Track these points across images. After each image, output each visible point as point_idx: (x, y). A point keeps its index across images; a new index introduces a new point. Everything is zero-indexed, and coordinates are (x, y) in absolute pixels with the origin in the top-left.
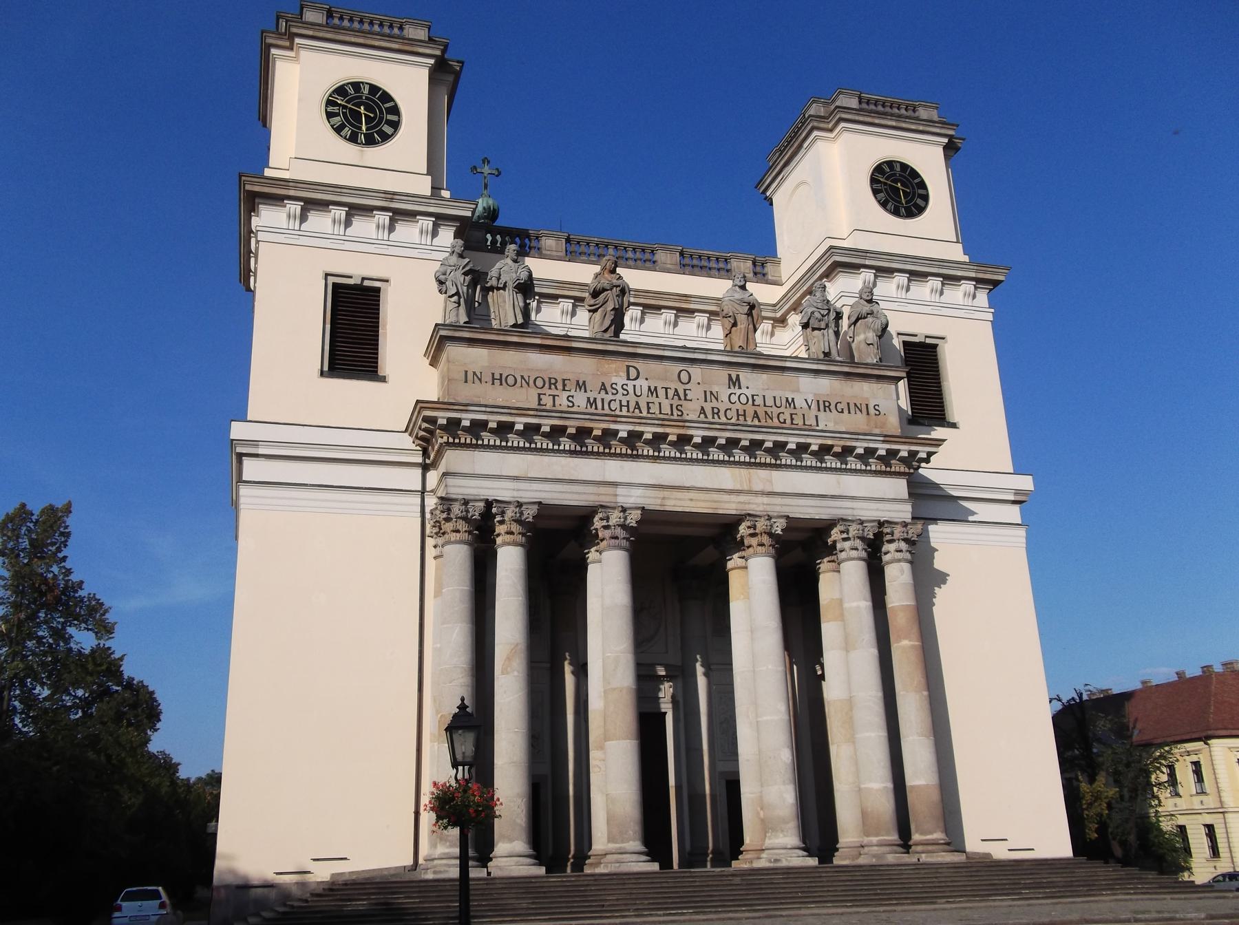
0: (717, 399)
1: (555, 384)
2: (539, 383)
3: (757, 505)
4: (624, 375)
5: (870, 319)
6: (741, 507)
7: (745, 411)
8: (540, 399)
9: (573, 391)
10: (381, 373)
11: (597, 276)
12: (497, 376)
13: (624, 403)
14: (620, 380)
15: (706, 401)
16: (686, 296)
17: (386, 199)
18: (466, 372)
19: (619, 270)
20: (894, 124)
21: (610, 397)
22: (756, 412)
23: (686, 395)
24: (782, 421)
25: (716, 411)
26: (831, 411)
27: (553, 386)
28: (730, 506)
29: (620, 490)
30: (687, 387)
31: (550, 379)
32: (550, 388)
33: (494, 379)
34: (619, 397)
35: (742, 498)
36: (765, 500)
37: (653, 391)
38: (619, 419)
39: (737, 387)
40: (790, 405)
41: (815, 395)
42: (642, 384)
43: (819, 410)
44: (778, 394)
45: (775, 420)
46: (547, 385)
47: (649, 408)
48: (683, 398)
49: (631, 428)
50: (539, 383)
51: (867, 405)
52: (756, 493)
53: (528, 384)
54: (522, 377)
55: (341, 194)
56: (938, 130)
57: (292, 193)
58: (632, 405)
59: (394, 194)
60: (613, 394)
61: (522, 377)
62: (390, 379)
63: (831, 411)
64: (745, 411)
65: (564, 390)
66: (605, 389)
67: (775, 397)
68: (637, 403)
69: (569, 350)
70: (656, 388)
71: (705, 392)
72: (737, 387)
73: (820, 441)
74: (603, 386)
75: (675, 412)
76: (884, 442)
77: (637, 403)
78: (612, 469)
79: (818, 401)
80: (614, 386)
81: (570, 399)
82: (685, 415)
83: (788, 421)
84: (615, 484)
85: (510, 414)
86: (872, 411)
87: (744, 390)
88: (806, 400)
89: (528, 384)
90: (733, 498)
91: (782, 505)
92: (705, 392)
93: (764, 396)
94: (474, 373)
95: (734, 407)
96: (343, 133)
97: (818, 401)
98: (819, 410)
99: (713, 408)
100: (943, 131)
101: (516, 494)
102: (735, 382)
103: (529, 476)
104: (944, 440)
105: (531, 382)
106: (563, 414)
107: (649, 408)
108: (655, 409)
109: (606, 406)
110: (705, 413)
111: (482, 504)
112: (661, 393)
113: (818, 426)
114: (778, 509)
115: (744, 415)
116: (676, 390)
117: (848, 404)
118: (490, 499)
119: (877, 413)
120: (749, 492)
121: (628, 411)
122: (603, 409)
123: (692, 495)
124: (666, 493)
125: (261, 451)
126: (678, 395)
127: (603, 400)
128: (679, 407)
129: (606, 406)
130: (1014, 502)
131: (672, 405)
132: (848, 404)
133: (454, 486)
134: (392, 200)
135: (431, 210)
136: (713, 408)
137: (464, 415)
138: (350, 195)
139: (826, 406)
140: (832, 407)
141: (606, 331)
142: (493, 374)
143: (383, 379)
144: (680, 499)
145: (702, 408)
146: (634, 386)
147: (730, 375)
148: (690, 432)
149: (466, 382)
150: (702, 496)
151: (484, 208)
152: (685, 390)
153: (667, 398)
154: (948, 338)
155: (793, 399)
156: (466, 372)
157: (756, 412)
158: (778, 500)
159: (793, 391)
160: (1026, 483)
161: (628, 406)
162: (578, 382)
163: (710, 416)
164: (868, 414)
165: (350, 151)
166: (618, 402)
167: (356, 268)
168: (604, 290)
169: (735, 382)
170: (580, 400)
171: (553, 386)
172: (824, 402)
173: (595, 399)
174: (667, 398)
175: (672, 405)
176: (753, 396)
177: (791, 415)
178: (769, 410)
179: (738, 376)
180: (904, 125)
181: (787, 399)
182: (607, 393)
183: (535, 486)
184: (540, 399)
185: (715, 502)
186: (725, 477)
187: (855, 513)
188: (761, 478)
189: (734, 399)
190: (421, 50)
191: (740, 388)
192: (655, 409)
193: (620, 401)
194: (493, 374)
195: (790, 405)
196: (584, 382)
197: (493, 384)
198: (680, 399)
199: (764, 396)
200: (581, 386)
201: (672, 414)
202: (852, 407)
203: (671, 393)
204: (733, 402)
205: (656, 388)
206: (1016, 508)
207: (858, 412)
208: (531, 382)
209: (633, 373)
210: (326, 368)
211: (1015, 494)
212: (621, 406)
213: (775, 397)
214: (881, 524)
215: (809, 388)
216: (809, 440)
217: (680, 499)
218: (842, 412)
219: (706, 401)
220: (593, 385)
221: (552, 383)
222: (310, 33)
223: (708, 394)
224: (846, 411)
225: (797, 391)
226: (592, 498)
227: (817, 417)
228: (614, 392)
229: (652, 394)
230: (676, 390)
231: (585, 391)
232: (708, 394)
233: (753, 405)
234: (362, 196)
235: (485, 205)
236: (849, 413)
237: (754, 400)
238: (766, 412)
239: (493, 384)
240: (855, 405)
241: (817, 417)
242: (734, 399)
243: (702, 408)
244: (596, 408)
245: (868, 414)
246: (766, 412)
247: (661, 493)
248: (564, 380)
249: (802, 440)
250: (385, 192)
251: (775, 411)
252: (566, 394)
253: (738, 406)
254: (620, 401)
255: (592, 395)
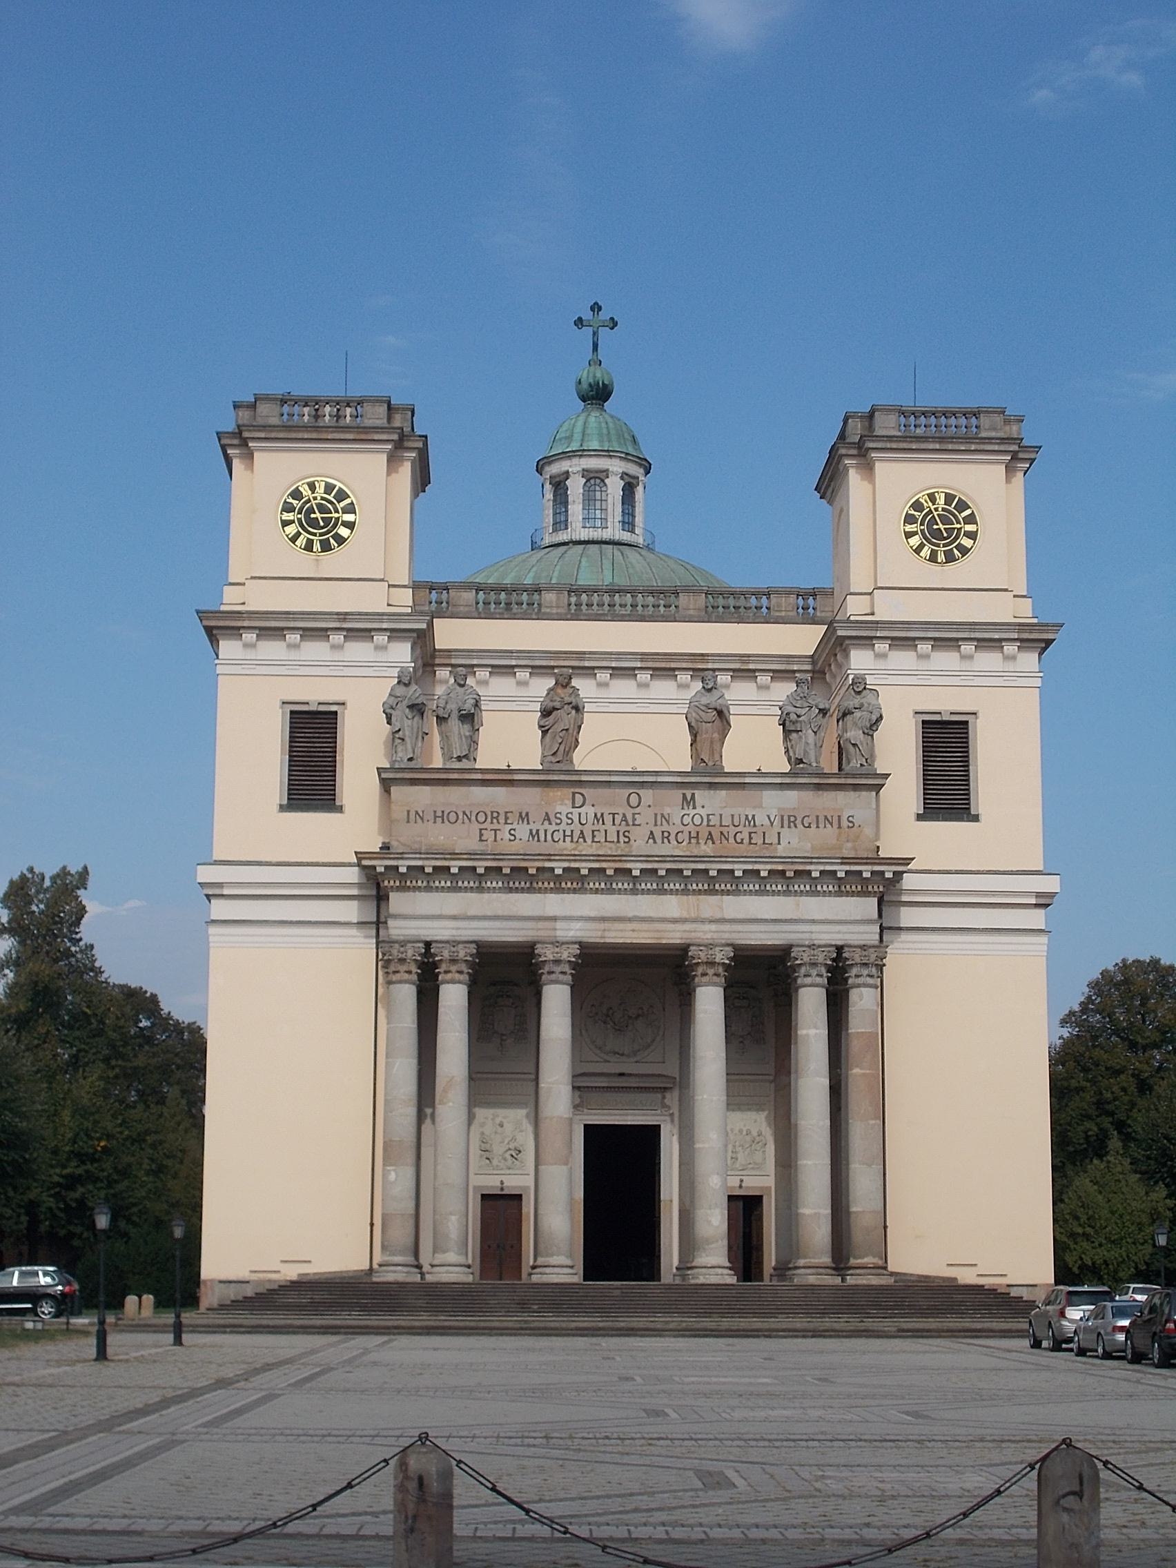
0: (668, 822)
1: (497, 818)
2: (481, 818)
3: (706, 933)
4: (569, 803)
5: (858, 714)
6: (685, 935)
7: (698, 833)
8: (481, 835)
9: (516, 823)
10: (338, 803)
11: (550, 690)
12: (439, 814)
13: (568, 833)
14: (564, 808)
15: (656, 825)
16: (702, 655)
17: (339, 620)
18: (408, 812)
19: (574, 683)
20: (937, 446)
21: (554, 827)
22: (710, 834)
23: (634, 819)
24: (739, 841)
25: (666, 834)
26: (796, 826)
27: (495, 821)
28: (674, 936)
29: (559, 925)
30: (637, 810)
31: (492, 812)
32: (492, 823)
33: (436, 817)
34: (562, 827)
35: (687, 927)
36: (713, 927)
37: (599, 818)
38: (553, 858)
39: (691, 807)
40: (750, 822)
41: (779, 809)
42: (588, 811)
43: (782, 827)
44: (736, 811)
45: (731, 840)
46: (489, 819)
47: (594, 836)
48: (631, 823)
49: (566, 865)
50: (481, 818)
51: (839, 816)
52: (703, 921)
53: (470, 820)
54: (464, 813)
55: (295, 620)
56: (996, 448)
57: (246, 624)
58: (577, 834)
59: (347, 614)
60: (557, 824)
61: (464, 813)
62: (346, 809)
63: (796, 826)
64: (698, 833)
65: (506, 823)
66: (549, 820)
67: (733, 816)
68: (582, 832)
69: (510, 783)
70: (602, 815)
71: (656, 815)
72: (691, 807)
73: (769, 867)
74: (547, 818)
75: (622, 839)
76: (842, 863)
77: (582, 832)
78: (553, 904)
79: (782, 817)
80: (558, 815)
81: (512, 832)
82: (632, 841)
83: (746, 841)
84: (554, 919)
85: (445, 859)
86: (845, 823)
87: (699, 810)
88: (769, 817)
89: (470, 820)
90: (679, 927)
91: (730, 932)
92: (656, 815)
93: (721, 815)
94: (417, 813)
95: (686, 829)
96: (298, 543)
97: (782, 817)
98: (782, 827)
99: (663, 832)
100: (1002, 448)
101: (454, 932)
102: (689, 802)
103: (469, 914)
104: (913, 859)
105: (473, 818)
106: (496, 856)
107: (594, 836)
108: (600, 837)
109: (549, 837)
110: (654, 838)
111: (421, 945)
112: (608, 819)
113: (779, 843)
114: (726, 936)
115: (697, 837)
116: (624, 815)
117: (817, 817)
118: (428, 939)
119: (851, 825)
120: (694, 921)
121: (572, 841)
122: (546, 841)
123: (635, 925)
124: (607, 925)
125: (226, 892)
126: (626, 821)
127: (546, 831)
128: (626, 834)
129: (549, 837)
130: (1037, 906)
131: (618, 832)
132: (817, 817)
133: (396, 928)
134: (344, 620)
135: (385, 626)
136: (663, 832)
137: (400, 863)
138: (302, 620)
139: (792, 823)
140: (798, 822)
141: (554, 754)
142: (435, 812)
143: (340, 809)
144: (621, 931)
145: (652, 833)
146: (580, 814)
147: (684, 795)
148: (628, 866)
149: (408, 822)
150: (645, 926)
151: (590, 385)
152: (634, 814)
153: (614, 824)
154: (980, 715)
155: (754, 816)
156: (408, 812)
157: (710, 834)
158: (727, 927)
159: (755, 807)
160: (1051, 884)
161: (572, 836)
162: (521, 813)
163: (659, 841)
164: (840, 827)
165: (303, 563)
166: (561, 832)
167: (314, 694)
168: (555, 709)
169: (689, 802)
170: (523, 831)
171: (495, 821)
172: (789, 816)
173: (538, 831)
174: (614, 824)
175: (618, 832)
176: (708, 815)
177: (750, 833)
178: (725, 830)
179: (693, 794)
180: (950, 447)
181: (747, 816)
182: (550, 824)
183: (475, 924)
184: (481, 835)
185: (658, 931)
186: (671, 905)
187: (814, 936)
188: (710, 905)
189: (687, 820)
190: (376, 437)
191: (694, 808)
192: (600, 837)
193: (564, 831)
194: (435, 812)
195: (750, 822)
196: (527, 814)
197: (435, 822)
198: (628, 825)
199: (721, 815)
200: (524, 817)
201: (618, 842)
202: (821, 819)
203: (618, 819)
204: (685, 823)
205: (602, 815)
206: (1042, 912)
207: (828, 825)
208: (473, 818)
209: (579, 798)
210: (285, 802)
211: (1037, 897)
212: (565, 836)
213: (733, 816)
214: (840, 949)
215: (774, 802)
216: (756, 867)
217: (621, 931)
218: (809, 827)
219: (656, 825)
220: (536, 816)
221: (495, 816)
222: (262, 435)
223: (659, 817)
224: (814, 826)
225: (761, 806)
226: (531, 933)
227: (779, 833)
228: (559, 821)
229: (598, 821)
230: (624, 815)
231: (528, 823)
232: (659, 817)
233: (708, 825)
234: (315, 620)
235: (591, 381)
236: (818, 827)
237: (709, 820)
238: (722, 833)
239: (435, 822)
240: (826, 817)
241: (779, 833)
242: (687, 820)
243: (652, 833)
244: (539, 841)
245: (840, 827)
246: (722, 833)
247: (602, 926)
248: (506, 813)
249: (749, 867)
250: (337, 614)
251: (733, 830)
252: (510, 827)
253: (691, 828)
254: (564, 831)
255: (534, 827)
